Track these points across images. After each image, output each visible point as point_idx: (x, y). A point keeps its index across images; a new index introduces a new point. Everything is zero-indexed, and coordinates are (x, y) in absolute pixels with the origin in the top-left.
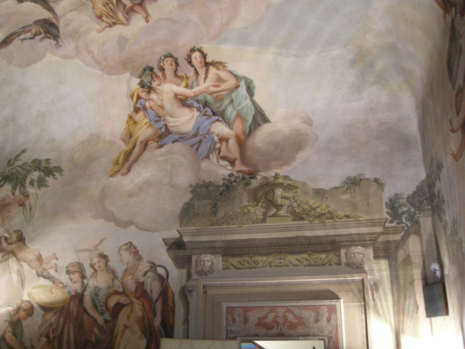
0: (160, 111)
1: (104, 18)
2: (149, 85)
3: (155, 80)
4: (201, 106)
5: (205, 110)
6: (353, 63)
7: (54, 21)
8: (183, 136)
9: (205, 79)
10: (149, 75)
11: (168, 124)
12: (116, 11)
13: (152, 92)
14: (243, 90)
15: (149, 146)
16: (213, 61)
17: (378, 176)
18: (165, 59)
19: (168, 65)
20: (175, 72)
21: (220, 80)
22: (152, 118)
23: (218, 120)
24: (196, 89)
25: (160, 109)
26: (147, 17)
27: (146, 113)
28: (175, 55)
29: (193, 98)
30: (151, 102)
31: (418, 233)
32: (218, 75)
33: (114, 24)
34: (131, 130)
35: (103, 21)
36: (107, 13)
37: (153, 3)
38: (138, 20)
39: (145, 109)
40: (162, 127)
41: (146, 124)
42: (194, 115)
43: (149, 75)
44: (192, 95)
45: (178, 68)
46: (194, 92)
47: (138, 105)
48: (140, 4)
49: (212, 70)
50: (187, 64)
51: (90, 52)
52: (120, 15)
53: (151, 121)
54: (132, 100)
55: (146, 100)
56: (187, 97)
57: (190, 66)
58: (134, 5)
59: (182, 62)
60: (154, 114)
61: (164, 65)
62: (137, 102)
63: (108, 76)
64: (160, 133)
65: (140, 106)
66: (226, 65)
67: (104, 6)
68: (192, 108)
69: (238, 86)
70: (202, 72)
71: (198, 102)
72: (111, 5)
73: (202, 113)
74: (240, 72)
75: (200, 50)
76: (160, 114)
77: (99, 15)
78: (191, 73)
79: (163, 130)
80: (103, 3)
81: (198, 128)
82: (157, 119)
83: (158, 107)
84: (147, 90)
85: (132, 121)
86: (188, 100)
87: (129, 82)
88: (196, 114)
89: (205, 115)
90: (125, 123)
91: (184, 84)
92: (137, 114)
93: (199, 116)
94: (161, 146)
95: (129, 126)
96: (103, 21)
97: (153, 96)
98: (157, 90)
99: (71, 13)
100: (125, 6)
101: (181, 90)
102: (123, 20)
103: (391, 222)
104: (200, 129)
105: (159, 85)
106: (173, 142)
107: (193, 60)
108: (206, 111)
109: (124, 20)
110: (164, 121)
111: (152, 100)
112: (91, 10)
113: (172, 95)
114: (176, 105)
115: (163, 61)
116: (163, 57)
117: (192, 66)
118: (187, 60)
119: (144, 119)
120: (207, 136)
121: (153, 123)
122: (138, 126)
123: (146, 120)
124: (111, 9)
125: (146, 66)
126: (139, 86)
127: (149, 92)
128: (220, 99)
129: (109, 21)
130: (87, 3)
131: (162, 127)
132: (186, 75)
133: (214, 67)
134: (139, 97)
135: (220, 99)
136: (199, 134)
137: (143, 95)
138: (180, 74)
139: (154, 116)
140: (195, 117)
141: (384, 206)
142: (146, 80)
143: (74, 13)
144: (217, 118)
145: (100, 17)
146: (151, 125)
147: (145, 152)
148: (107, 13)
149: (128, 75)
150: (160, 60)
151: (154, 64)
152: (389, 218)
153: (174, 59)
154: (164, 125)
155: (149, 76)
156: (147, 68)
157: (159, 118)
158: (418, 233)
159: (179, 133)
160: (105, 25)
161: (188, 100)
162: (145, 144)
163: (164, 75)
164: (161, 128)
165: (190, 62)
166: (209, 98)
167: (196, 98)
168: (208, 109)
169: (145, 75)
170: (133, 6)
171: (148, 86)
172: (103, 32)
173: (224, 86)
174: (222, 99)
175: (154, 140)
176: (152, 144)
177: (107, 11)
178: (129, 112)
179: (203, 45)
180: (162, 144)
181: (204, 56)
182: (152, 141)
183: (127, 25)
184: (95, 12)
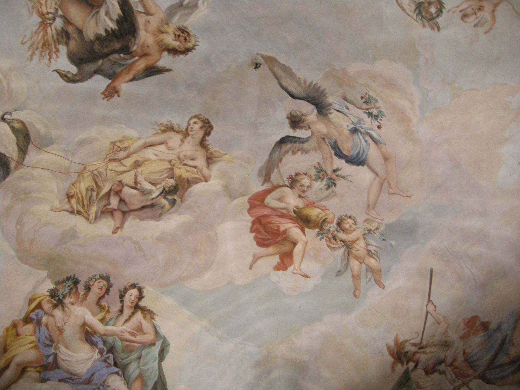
0: (56, 335)
1: (73, 201)
2: (61, 298)
3: (72, 295)
4: (105, 349)
5: (107, 355)
6: (258, 364)
7: (13, 165)
8: (74, 377)
9: (127, 321)
10: (69, 286)
11: (59, 354)
12: (94, 203)
13: (60, 307)
14: (156, 350)
15: (28, 373)
16: (145, 306)
18: (99, 279)
19: (97, 288)
20: (101, 298)
21: (140, 329)
22: (43, 338)
23: (117, 373)
24: (110, 328)
25: (57, 333)
26: (118, 228)
27: (37, 329)
28: (112, 280)
29: (102, 336)
30: (51, 319)
32: (141, 323)
33: (79, 213)
34: (8, 342)
35: (69, 202)
36: (82, 197)
37: (138, 220)
38: (106, 226)
39: (39, 323)
40: (50, 355)
41: (30, 343)
42: (92, 357)
43: (69, 286)
44: (103, 332)
45: (106, 295)
46: (106, 330)
47: (33, 315)
48: (124, 213)
49: (139, 315)
50: (118, 296)
51: (20, 222)
52: (94, 210)
53: (39, 341)
54: (29, 305)
55: (46, 313)
56: (95, 332)
57: (119, 300)
58: (119, 209)
59: (114, 292)
60: (46, 335)
61: (93, 285)
62: (33, 310)
63: (19, 262)
64: (45, 363)
65: (35, 317)
66: (155, 317)
67: (87, 190)
68: (94, 347)
69: (153, 344)
70: (127, 312)
71: (105, 343)
72: (95, 194)
73: (103, 358)
74: (163, 331)
75: (140, 290)
76: (55, 338)
77: (72, 194)
78: (115, 309)
79: (51, 360)
80: (89, 186)
81: (93, 374)
82: (48, 343)
83: (55, 328)
84: (55, 302)
85: (14, 331)
86: (95, 336)
87: (39, 283)
88: (96, 355)
89: (105, 361)
90: (3, 330)
91: (100, 316)
92: (25, 325)
93: (98, 359)
94: (43, 381)
95: (7, 335)
96: (69, 202)
97: (58, 313)
98: (66, 309)
99: (44, 171)
100: (109, 204)
101: (94, 321)
102: (91, 215)
104: (95, 377)
105: (72, 304)
106: (60, 381)
107: (127, 296)
108: (108, 358)
109: (92, 216)
110: (55, 349)
111: (53, 316)
112: (67, 184)
113: (80, 322)
114: (78, 335)
115: (96, 280)
116: (98, 276)
117: (122, 301)
118: (121, 292)
119: (32, 335)
120: (101, 387)
121: (41, 346)
122: (20, 341)
123: (33, 338)
124: (91, 197)
125: (72, 276)
126: (48, 294)
127: (55, 306)
128: (129, 350)
129: (75, 207)
130: (72, 174)
131: (50, 355)
132: (109, 307)
133: (142, 313)
134: (39, 306)
135: (129, 350)
136: (93, 382)
137: (47, 306)
138: (103, 303)
139: (46, 338)
140: (93, 359)
142: (61, 291)
143: (46, 173)
144: (117, 370)
145: (69, 197)
146: (36, 347)
147: (22, 381)
148: (82, 197)
149: (44, 273)
150: (93, 278)
151: (83, 279)
153: (108, 285)
154: (53, 353)
155: (68, 287)
156: (72, 278)
157: (51, 342)
159: (68, 372)
160: (67, 207)
161: (95, 336)
162: (23, 370)
163: (86, 296)
164: (48, 356)
165: (122, 297)
166: (119, 344)
167: (104, 337)
168: (111, 356)
169: (64, 284)
170: (115, 210)
171: (59, 299)
172: (57, 213)
173: (140, 338)
174: (131, 351)
175: (36, 368)
176: (32, 373)
177: (84, 196)
178: (16, 318)
179: (147, 287)
180: (46, 378)
181: (140, 297)
182: (33, 369)
183: (90, 223)
184: (70, 188)
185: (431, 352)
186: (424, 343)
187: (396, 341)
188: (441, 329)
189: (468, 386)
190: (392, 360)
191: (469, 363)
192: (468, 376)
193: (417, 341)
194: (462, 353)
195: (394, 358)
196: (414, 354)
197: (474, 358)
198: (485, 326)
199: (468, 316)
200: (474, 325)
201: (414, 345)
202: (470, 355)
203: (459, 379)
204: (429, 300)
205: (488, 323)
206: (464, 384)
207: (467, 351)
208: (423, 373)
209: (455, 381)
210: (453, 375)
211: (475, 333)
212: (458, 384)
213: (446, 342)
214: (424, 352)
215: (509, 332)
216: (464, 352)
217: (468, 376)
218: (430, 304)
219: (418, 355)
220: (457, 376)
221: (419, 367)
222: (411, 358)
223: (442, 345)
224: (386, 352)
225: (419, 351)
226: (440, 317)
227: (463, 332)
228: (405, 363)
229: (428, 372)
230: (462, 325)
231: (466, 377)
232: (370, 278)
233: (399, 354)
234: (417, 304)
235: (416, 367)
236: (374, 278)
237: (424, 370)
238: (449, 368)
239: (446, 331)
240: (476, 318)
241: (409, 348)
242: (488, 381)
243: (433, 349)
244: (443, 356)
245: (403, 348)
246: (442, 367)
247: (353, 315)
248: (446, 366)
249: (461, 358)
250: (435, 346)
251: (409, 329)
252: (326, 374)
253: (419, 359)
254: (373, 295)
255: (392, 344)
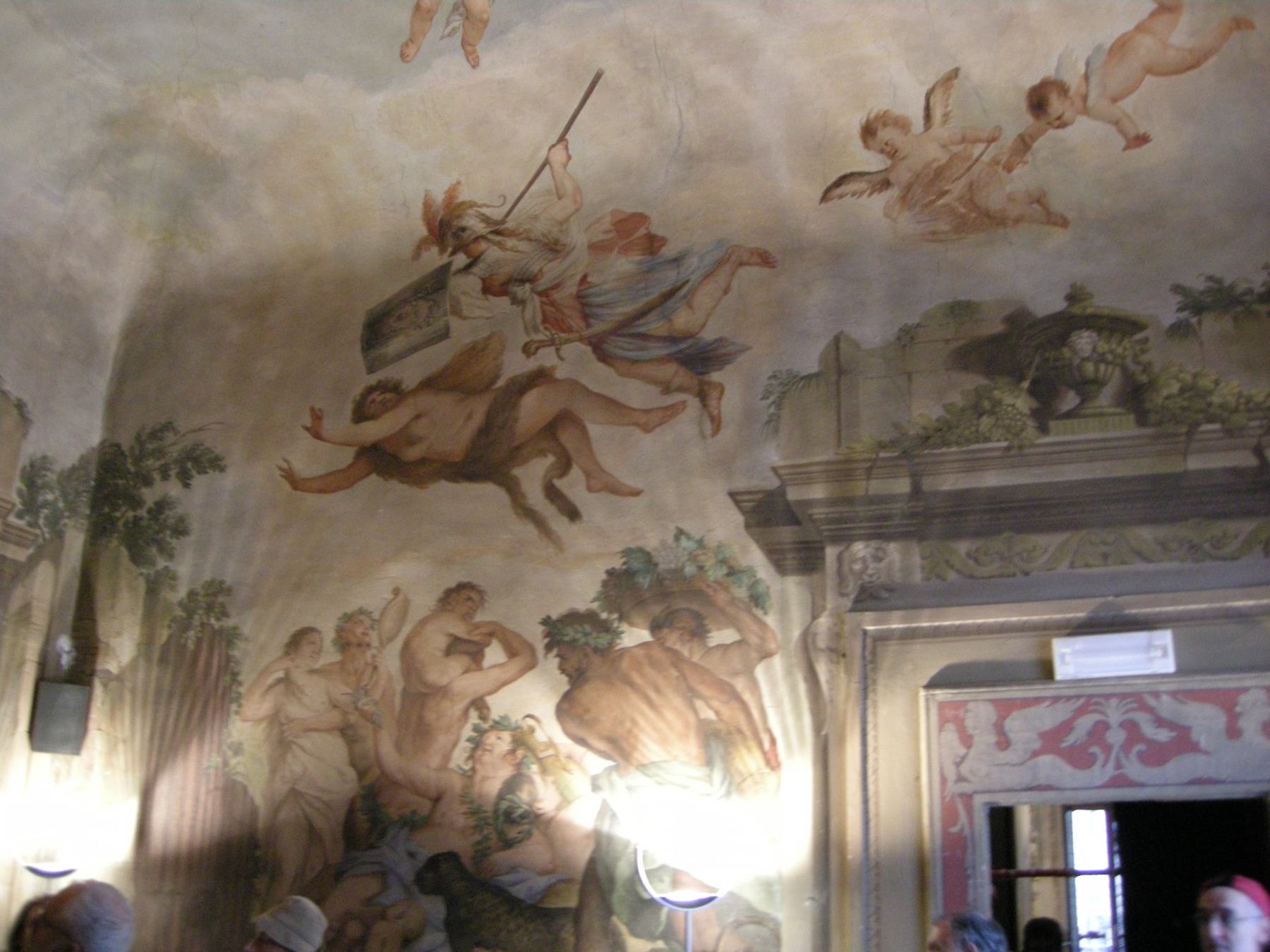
6: (110, 122)
17: (25, 397)
31: (56, 560)
103: (20, 516)
141: (18, 473)
152: (19, 506)
158: (56, 560)
185: (512, 250)
186: (510, 224)
187: (451, 194)
188: (559, 210)
189: (558, 350)
190: (423, 231)
191: (584, 305)
192: (569, 330)
193: (496, 214)
194: (578, 278)
195: (430, 230)
196: (478, 239)
197: (600, 300)
198: (653, 244)
199: (629, 208)
200: (633, 232)
201: (486, 220)
202: (591, 291)
203: (546, 329)
204: (562, 139)
205: (663, 241)
206: (552, 342)
207: (589, 279)
208: (478, 285)
209: (536, 330)
210: (539, 320)
211: (625, 250)
212: (541, 337)
213: (557, 242)
214: (499, 244)
215: (693, 278)
216: (584, 279)
217: (569, 330)
218: (560, 147)
219: (483, 245)
220: (545, 320)
221: (475, 270)
222: (467, 245)
223: (545, 244)
224: (417, 210)
225: (490, 237)
226: (569, 186)
227: (602, 237)
228: (450, 249)
229: (488, 288)
230: (607, 223)
231: (564, 331)
232: (454, 30)
233: (445, 227)
234: (532, 134)
235: (467, 268)
236: (465, 33)
237: (484, 280)
238: (537, 300)
239: (566, 220)
240: (641, 218)
241: (473, 223)
242: (604, 357)
243: (523, 246)
244: (536, 268)
245: (460, 216)
246: (523, 291)
247: (378, 99)
248: (532, 291)
249: (571, 288)
250: (530, 240)
251: (489, 183)
252: (265, 205)
253: (482, 253)
254: (444, 73)
255: (439, 197)
